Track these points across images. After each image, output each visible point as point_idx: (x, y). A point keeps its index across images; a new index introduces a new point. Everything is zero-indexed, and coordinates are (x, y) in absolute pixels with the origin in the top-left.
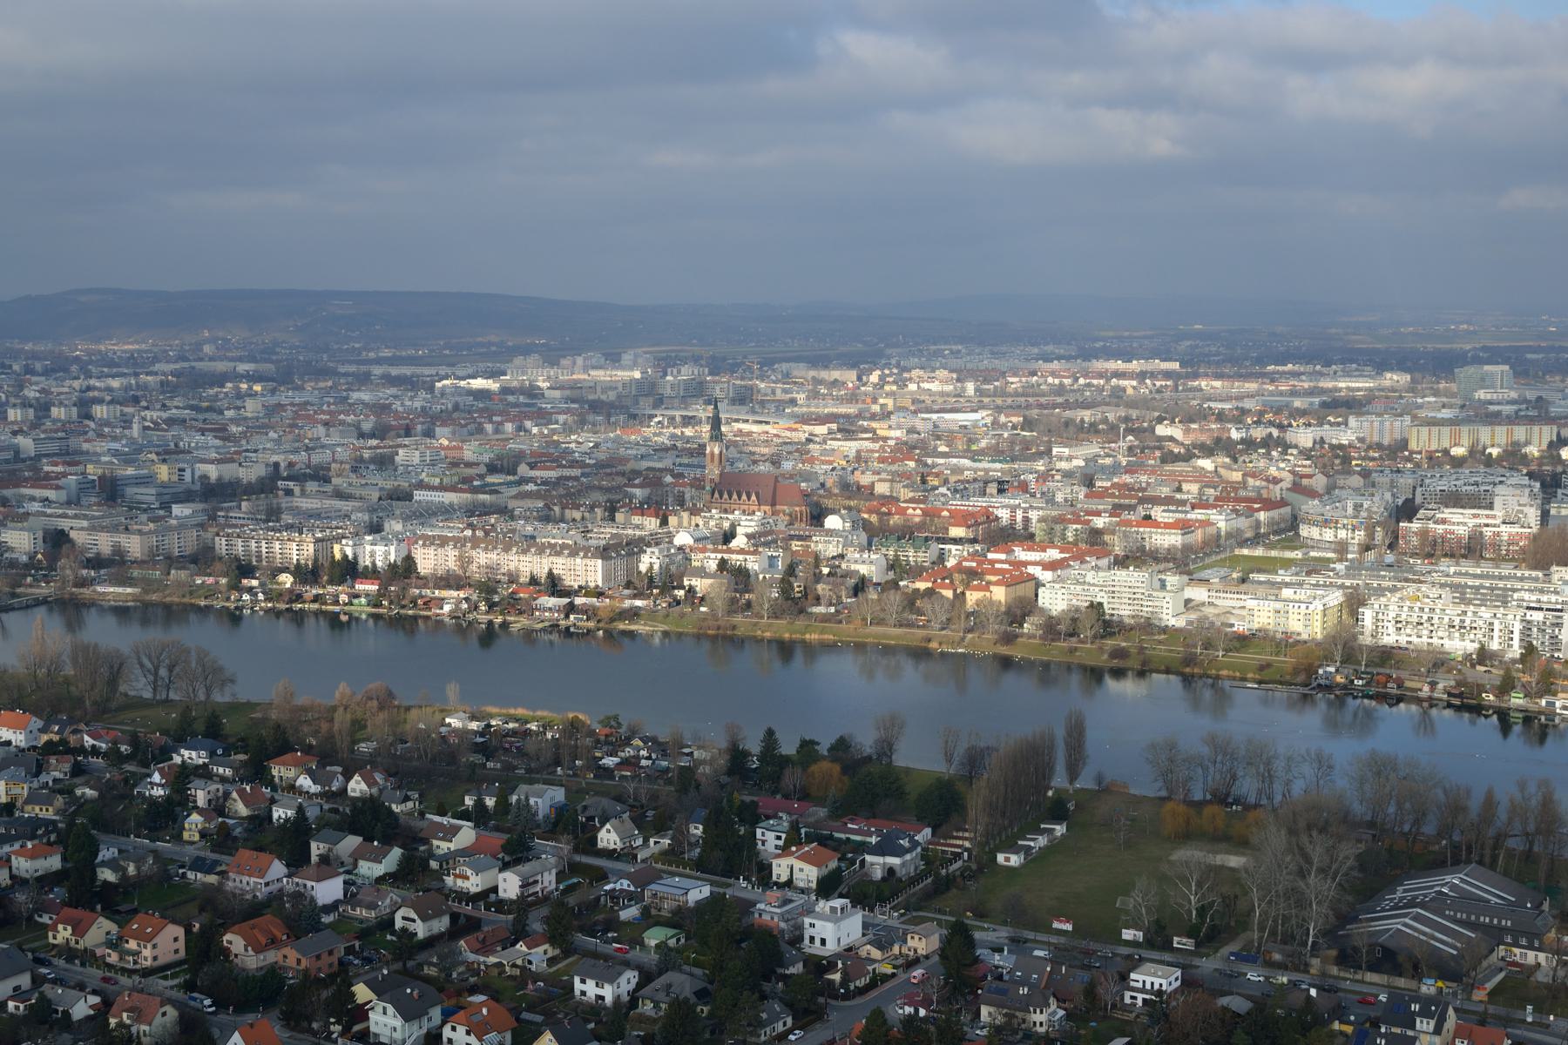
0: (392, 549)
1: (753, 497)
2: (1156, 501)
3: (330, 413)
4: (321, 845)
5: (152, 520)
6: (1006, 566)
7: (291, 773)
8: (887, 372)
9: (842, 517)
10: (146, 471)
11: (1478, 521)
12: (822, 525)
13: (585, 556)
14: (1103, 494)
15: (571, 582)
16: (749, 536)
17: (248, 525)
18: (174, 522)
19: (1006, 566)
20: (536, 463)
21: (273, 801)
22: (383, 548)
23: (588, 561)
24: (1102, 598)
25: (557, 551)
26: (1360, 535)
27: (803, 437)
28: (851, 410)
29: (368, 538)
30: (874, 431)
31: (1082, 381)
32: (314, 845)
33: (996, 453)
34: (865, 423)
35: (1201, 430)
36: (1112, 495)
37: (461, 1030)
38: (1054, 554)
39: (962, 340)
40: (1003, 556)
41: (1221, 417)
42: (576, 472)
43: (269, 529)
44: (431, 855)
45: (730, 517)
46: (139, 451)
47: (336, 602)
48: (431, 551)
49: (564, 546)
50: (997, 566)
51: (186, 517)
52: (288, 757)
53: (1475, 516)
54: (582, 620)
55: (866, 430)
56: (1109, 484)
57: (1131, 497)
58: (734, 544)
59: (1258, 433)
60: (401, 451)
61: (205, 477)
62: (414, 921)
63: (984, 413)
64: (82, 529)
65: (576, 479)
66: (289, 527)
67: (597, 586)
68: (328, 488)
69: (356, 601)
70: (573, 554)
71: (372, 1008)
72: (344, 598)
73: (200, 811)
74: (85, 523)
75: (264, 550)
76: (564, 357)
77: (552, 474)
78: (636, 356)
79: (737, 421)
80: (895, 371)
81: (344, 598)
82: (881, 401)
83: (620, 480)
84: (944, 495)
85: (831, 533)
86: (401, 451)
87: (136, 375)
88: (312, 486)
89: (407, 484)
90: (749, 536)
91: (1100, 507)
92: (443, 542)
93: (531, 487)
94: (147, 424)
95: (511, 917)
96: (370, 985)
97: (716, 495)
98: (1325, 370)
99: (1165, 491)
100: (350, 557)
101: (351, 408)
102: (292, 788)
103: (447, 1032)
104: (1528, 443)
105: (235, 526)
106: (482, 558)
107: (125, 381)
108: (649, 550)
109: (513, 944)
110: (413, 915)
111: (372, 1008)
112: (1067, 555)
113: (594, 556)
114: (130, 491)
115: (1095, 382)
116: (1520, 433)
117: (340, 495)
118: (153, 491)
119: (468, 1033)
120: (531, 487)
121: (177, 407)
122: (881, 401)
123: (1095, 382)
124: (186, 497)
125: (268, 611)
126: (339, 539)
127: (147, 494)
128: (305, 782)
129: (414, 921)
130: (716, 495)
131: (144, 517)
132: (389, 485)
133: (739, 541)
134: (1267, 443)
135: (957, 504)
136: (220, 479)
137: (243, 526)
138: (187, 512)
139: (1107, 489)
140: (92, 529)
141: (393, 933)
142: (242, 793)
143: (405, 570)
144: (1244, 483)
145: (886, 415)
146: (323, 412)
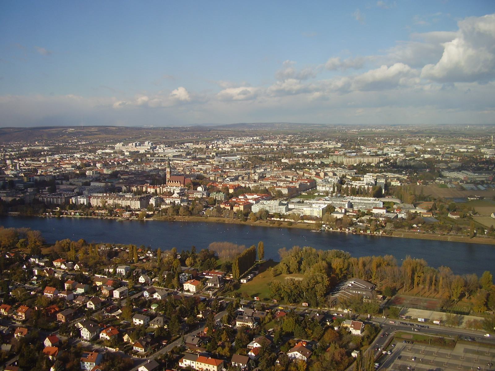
0: (85, 199)
1: (179, 182)
2: (281, 181)
3: (69, 160)
4: (68, 284)
5: (23, 193)
6: (244, 200)
7: (59, 264)
8: (214, 145)
9: (202, 187)
10: (21, 179)
11: (360, 184)
12: (197, 190)
13: (135, 200)
14: (268, 179)
15: (132, 207)
16: (178, 193)
17: (47, 194)
18: (28, 194)
19: (244, 200)
20: (123, 174)
21: (55, 272)
22: (82, 199)
23: (135, 202)
24: (268, 209)
25: (128, 199)
26: (332, 189)
27: (192, 164)
28: (204, 156)
29: (79, 197)
30: (210, 162)
31: (263, 147)
32: (66, 284)
33: (243, 167)
34: (208, 160)
35: (293, 160)
36: (270, 180)
37: (105, 334)
38: (255, 196)
39: (233, 136)
40: (243, 197)
41: (298, 157)
42: (133, 176)
43: (53, 195)
44: (96, 286)
45: (173, 188)
46: (19, 173)
47: (71, 215)
48: (95, 200)
49: (130, 198)
50: (241, 200)
51: (31, 192)
52: (58, 260)
53: (359, 183)
54: (134, 218)
55: (207, 162)
56: (269, 176)
57: (275, 180)
58: (173, 196)
59: (307, 161)
60: (87, 171)
61: (36, 180)
62: (92, 305)
63: (238, 156)
64: (4, 196)
65: (133, 178)
66: (58, 194)
67: (139, 208)
68: (68, 183)
69: (76, 214)
70: (132, 200)
71: (81, 330)
72: (73, 213)
73: (36, 276)
74: (5, 195)
75: (52, 201)
76: (130, 143)
77: (127, 177)
78: (149, 142)
79: (175, 160)
80: (216, 145)
81: (73, 213)
82: (212, 154)
83: (145, 178)
84: (228, 180)
85: (199, 192)
86: (87, 171)
87: (18, 151)
88: (64, 182)
89: (89, 181)
90: (178, 193)
91: (268, 183)
92: (98, 197)
93: (121, 181)
94: (21, 165)
95: (117, 302)
96: (81, 323)
97: (169, 182)
98: (324, 143)
99: (284, 178)
100: (74, 203)
101: (74, 159)
102: (60, 268)
103: (101, 335)
104: (372, 163)
105: (44, 194)
106: (110, 202)
107: (15, 153)
108: (152, 198)
109: (118, 310)
110: (92, 303)
111: (81, 330)
112: (259, 197)
113: (137, 200)
114: (17, 185)
115: (267, 147)
116: (371, 160)
117: (71, 184)
118: (22, 185)
119: (106, 335)
120: (121, 181)
121: (29, 160)
122: (212, 154)
123: (267, 147)
124: (31, 186)
125: (52, 217)
126: (71, 197)
127: (21, 186)
128: (63, 266)
129: (92, 305)
130: (169, 182)
131: (20, 192)
132: (84, 181)
133: (175, 195)
134: (309, 163)
135: (231, 183)
136: (40, 180)
137: (46, 194)
138: (32, 190)
139: (269, 177)
140: (7, 196)
141: (87, 308)
142: (47, 270)
143: (89, 205)
144: (304, 175)
145: (213, 158)
146: (67, 160)
